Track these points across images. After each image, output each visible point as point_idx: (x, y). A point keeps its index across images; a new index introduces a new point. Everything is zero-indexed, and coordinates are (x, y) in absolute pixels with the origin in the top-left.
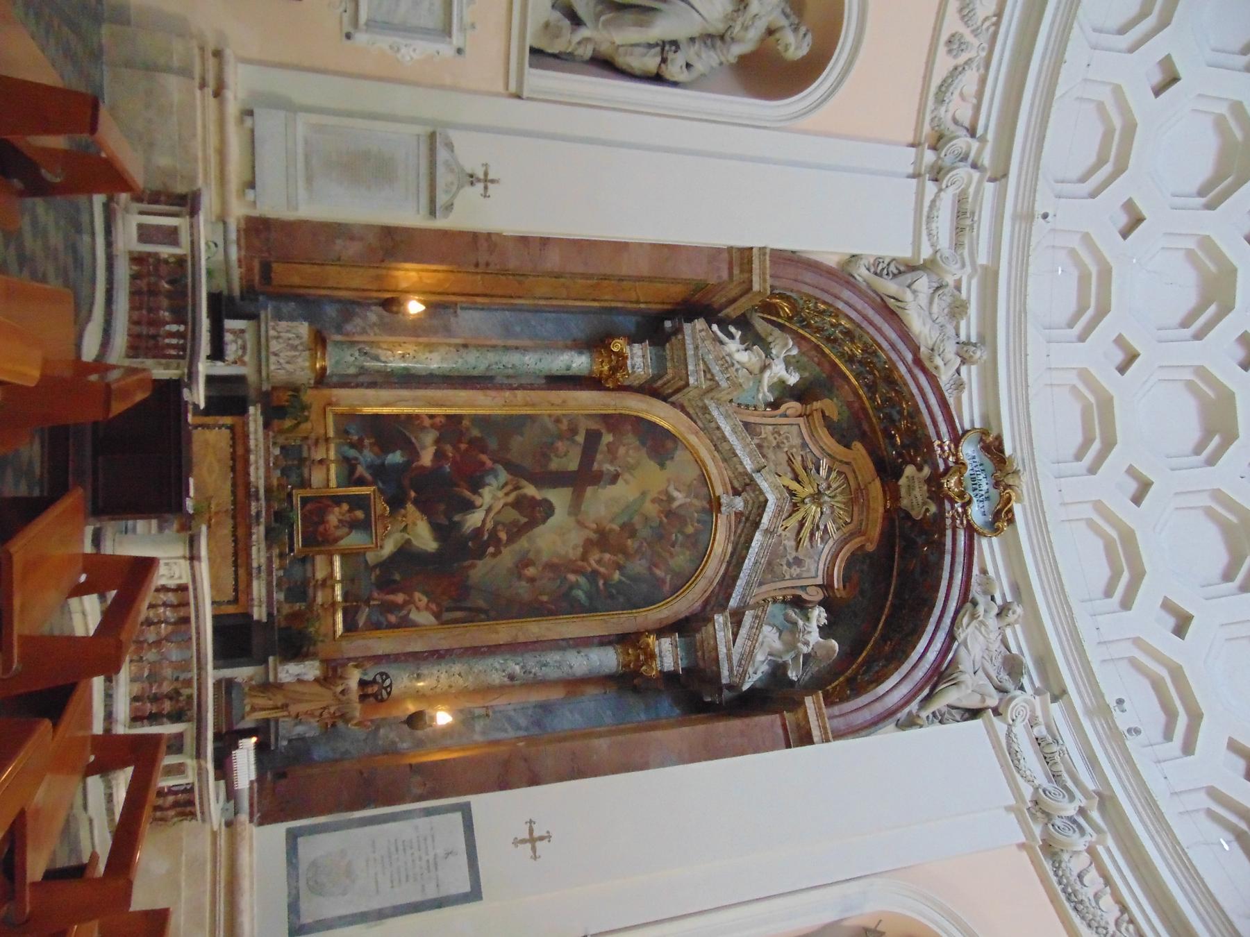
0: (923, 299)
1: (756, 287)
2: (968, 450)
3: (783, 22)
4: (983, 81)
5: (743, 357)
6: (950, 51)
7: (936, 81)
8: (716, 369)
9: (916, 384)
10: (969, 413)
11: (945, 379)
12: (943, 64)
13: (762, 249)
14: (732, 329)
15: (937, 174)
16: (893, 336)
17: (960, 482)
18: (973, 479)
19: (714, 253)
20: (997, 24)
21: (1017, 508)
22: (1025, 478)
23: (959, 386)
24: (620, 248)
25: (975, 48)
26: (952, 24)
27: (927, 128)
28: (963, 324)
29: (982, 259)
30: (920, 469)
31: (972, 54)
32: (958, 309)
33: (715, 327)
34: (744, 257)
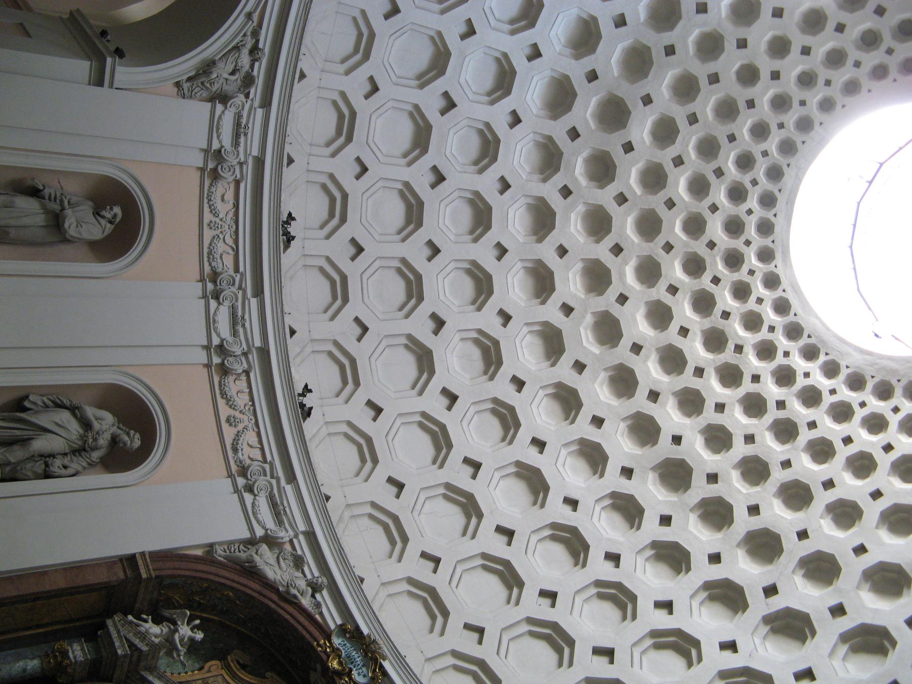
0: (272, 561)
1: (144, 576)
2: (337, 641)
3: (119, 431)
4: (259, 434)
5: (155, 629)
6: (231, 425)
7: (228, 442)
8: (136, 641)
9: (286, 612)
10: (332, 618)
11: (306, 602)
12: (229, 433)
13: (143, 554)
14: (145, 616)
15: (250, 489)
16: (257, 587)
17: (340, 663)
18: (349, 657)
19: (110, 563)
20: (253, 405)
21: (386, 665)
22: (380, 642)
23: (318, 605)
24: (41, 573)
25: (246, 420)
26: (225, 411)
27: (234, 468)
28: (306, 569)
29: (302, 527)
30: (315, 670)
31: (246, 423)
32: (299, 562)
33: (130, 617)
34: (131, 560)
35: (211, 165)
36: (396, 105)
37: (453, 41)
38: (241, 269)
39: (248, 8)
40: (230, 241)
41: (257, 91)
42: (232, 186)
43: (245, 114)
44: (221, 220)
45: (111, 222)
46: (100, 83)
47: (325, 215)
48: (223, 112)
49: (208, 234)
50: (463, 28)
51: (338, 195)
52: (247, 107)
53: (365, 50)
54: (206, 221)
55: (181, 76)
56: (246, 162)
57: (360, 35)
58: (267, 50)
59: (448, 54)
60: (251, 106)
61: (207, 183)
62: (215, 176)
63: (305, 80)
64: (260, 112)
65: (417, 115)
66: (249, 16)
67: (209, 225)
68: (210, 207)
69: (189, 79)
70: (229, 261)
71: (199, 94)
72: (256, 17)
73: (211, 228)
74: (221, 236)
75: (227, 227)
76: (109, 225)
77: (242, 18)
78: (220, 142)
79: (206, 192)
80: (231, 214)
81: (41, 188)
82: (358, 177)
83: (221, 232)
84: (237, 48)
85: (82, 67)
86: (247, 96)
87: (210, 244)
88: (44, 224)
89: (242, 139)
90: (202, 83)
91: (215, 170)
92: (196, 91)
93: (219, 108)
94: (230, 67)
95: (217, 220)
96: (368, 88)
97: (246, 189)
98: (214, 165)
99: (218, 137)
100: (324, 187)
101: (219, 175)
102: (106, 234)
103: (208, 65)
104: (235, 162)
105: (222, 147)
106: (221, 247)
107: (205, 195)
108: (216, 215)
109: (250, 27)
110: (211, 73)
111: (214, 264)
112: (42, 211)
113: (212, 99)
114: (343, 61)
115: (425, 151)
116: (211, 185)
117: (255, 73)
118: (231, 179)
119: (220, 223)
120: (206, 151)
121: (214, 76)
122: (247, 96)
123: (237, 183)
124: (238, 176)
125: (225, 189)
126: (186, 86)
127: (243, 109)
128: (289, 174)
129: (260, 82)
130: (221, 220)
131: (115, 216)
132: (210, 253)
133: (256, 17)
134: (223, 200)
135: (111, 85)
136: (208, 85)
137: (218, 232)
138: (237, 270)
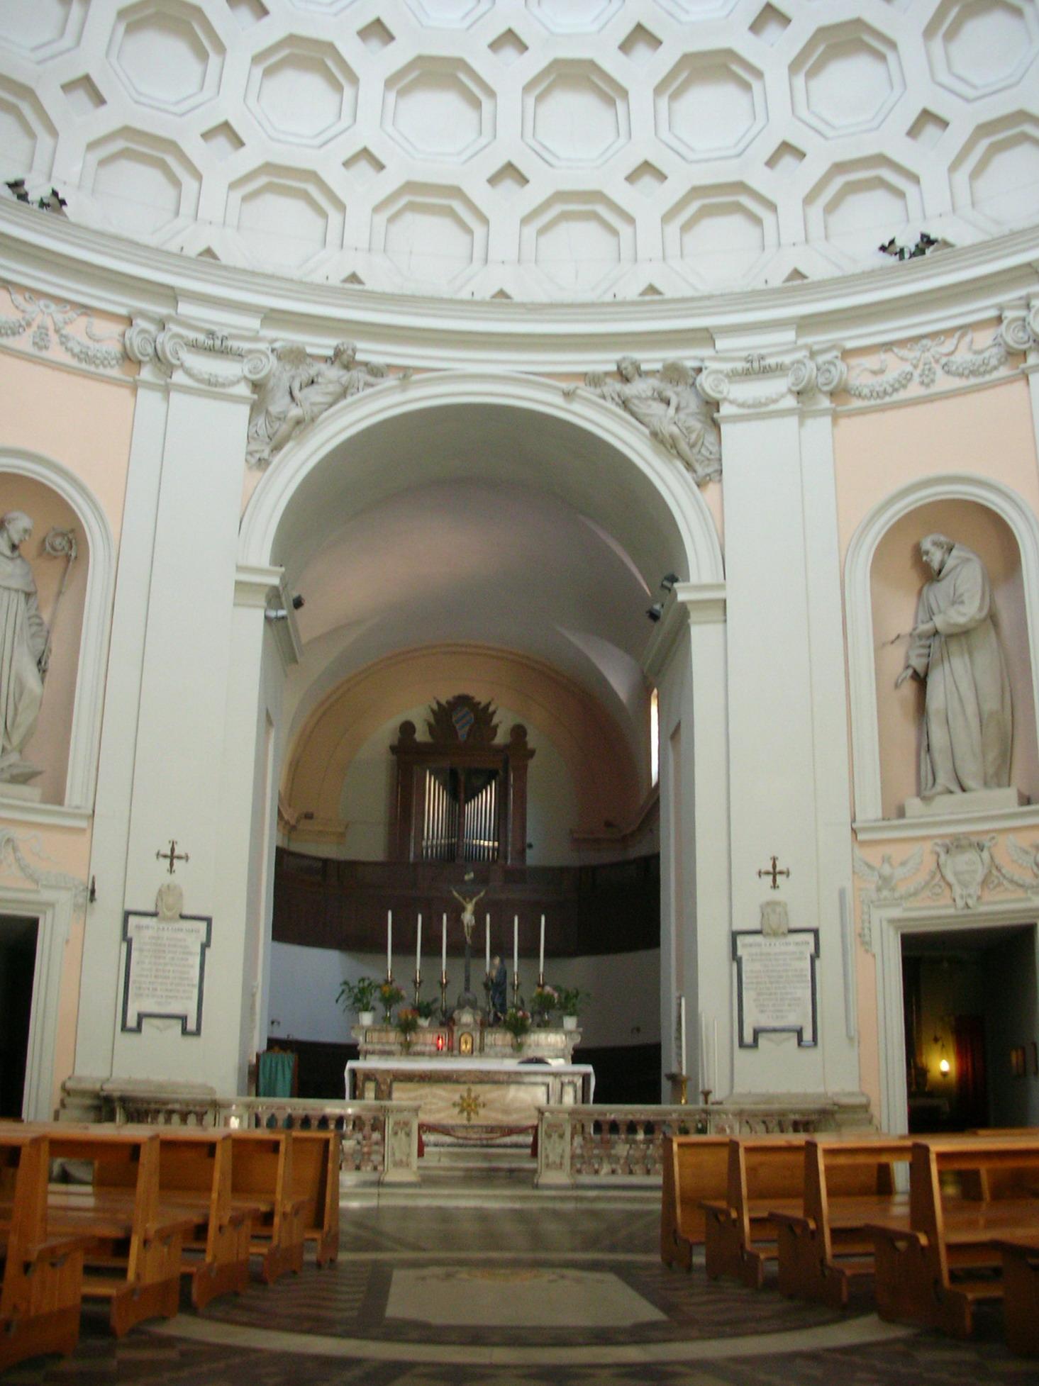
35: (825, 403)
36: (663, 125)
37: (533, 63)
38: (993, 313)
39: (559, 400)
40: (949, 345)
41: (687, 357)
42: (853, 362)
43: (727, 367)
44: (915, 367)
45: (950, 550)
47: (879, 195)
48: (732, 402)
49: (944, 383)
50: (509, 53)
51: (838, 182)
53: (586, 202)
54: (922, 391)
55: (686, 482)
56: (806, 346)
57: (565, 216)
58: (617, 356)
59: (557, 64)
61: (856, 403)
62: (840, 392)
63: (658, 285)
65: (672, 85)
66: (568, 395)
67: (928, 385)
68: (895, 390)
69: (689, 466)
70: (984, 338)
71: (711, 448)
72: (564, 385)
73: (933, 381)
74: (944, 360)
75: (927, 354)
76: (954, 552)
77: (576, 407)
78: (783, 396)
79: (872, 402)
80: (903, 352)
81: (910, 672)
82: (801, 155)
83: (937, 361)
84: (625, 404)
86: (699, 370)
87: (961, 375)
88: (967, 657)
89: (771, 361)
90: (692, 446)
91: (832, 394)
92: (707, 454)
93: (726, 410)
94: (658, 408)
95: (917, 373)
96: (647, 180)
97: (854, 337)
98: (826, 395)
99: (775, 401)
100: (831, 208)
101: (836, 387)
102: (971, 556)
103: (662, 442)
104: (811, 365)
105: (790, 391)
106: (963, 357)
107: (879, 401)
108: (908, 377)
109: (585, 391)
110: (672, 436)
111: (994, 362)
112: (946, 665)
113: (716, 425)
114: (614, 232)
115: (730, 54)
116: (859, 396)
117: (658, 366)
118: (841, 366)
119: (921, 367)
120: (803, 415)
121: (675, 430)
122: (699, 370)
123: (846, 354)
124: (836, 353)
125: (860, 374)
126: (701, 470)
127: (720, 372)
128: (817, 270)
129: (671, 355)
130: (915, 367)
131: (935, 544)
132: (973, 373)
133: (564, 385)
134: (882, 371)
135: (721, 587)
137: (939, 371)
138: (999, 320)
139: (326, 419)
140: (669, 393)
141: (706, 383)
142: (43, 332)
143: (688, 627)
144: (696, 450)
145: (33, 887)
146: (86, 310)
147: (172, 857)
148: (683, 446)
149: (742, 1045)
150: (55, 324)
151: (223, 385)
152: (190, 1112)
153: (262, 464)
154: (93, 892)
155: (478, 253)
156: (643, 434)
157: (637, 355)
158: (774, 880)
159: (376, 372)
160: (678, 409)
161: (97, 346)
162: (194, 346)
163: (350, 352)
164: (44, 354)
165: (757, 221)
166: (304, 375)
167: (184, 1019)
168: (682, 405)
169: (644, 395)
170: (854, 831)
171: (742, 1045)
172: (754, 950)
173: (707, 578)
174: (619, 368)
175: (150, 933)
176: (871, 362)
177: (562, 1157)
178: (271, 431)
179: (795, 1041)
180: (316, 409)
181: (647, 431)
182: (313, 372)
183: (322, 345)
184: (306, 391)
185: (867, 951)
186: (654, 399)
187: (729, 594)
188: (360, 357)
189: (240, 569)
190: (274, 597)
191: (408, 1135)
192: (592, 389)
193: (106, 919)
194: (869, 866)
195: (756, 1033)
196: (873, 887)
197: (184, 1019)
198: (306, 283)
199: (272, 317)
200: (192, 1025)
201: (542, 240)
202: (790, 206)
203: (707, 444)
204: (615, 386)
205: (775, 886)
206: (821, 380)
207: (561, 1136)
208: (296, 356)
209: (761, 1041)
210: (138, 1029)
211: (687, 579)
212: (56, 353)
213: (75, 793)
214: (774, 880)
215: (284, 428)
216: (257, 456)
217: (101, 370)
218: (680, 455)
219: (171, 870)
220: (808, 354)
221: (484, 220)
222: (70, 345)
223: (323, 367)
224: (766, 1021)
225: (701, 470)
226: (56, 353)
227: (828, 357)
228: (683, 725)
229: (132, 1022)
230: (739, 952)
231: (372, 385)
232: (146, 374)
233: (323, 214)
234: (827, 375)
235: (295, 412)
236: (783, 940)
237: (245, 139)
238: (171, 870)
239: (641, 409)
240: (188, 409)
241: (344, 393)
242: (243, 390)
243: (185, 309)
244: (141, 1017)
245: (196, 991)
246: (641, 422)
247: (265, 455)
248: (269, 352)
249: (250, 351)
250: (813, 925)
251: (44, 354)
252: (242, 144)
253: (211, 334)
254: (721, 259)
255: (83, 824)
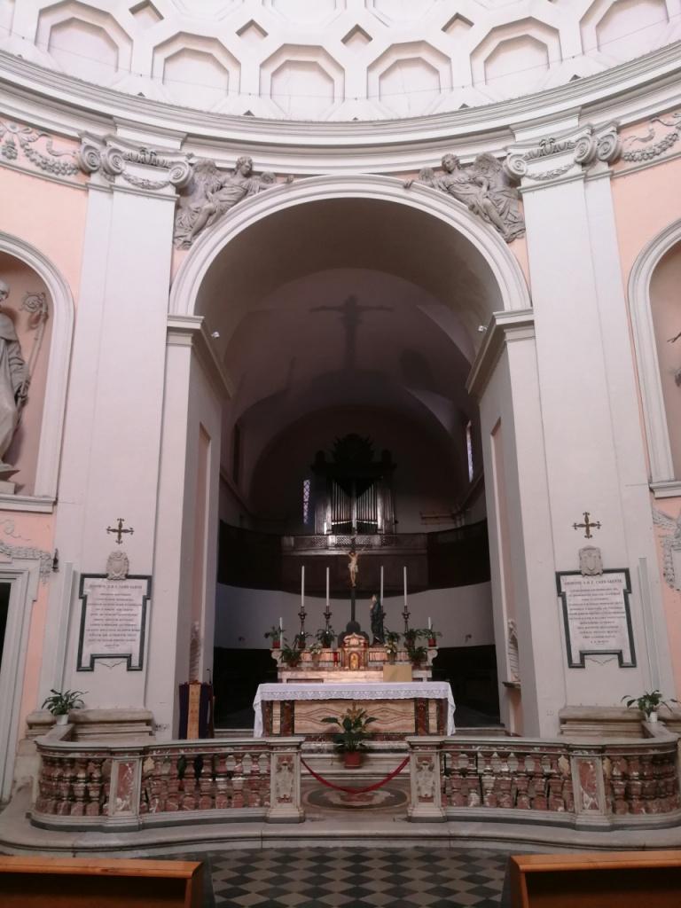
35: (604, 167)
39: (401, 192)
41: (494, 149)
42: (626, 134)
43: (524, 152)
46: (531, 323)
48: (529, 177)
52: (514, 151)
57: (398, 63)
58: (440, 155)
60: (515, 146)
64: (521, 136)
66: (407, 187)
68: (665, 150)
69: (499, 228)
72: (405, 180)
78: (570, 167)
84: (449, 189)
85: (516, 351)
86: (503, 159)
89: (560, 142)
92: (513, 220)
93: (525, 183)
94: (473, 189)
97: (625, 114)
98: (602, 161)
99: (565, 171)
110: (485, 206)
113: (520, 198)
116: (633, 160)
120: (586, 179)
121: (488, 202)
125: (631, 143)
127: (521, 155)
134: (651, 138)
135: (530, 311)
136: (502, 206)
139: (231, 214)
140: (481, 178)
141: (511, 164)
142: (11, 146)
143: (505, 344)
144: (503, 217)
145: (9, 560)
146: (47, 132)
147: (120, 531)
148: (494, 214)
149: (571, 665)
150: (20, 141)
151: (154, 188)
152: (89, 760)
153: (187, 244)
154: (56, 561)
155: (338, 93)
156: (463, 209)
157: (458, 153)
158: (588, 531)
159: (268, 179)
160: (488, 188)
161: (56, 159)
162: (130, 160)
163: (247, 164)
164: (12, 162)
165: (542, 46)
166: (215, 182)
167: (129, 657)
168: (492, 185)
169: (463, 181)
170: (651, 490)
171: (571, 665)
172: (577, 587)
173: (517, 306)
174: (443, 162)
175: (101, 590)
176: (642, 131)
177: (433, 789)
178: (192, 221)
179: (617, 661)
180: (224, 204)
181: (466, 207)
182: (221, 179)
183: (227, 159)
184: (217, 194)
185: (672, 587)
186: (471, 183)
187: (535, 317)
188: (256, 169)
189: (170, 318)
190: (196, 335)
191: (290, 770)
192: (424, 182)
193: (60, 584)
194: (670, 518)
195: (583, 655)
196: (672, 533)
197: (129, 657)
198: (212, 114)
199: (188, 139)
200: (135, 662)
201: (383, 82)
202: (569, 30)
203: (511, 211)
204: (441, 177)
205: (588, 536)
206: (601, 151)
207: (431, 769)
208: (210, 168)
209: (588, 662)
210: (91, 668)
211: (502, 308)
212: (23, 161)
213: (43, 485)
214: (588, 531)
215: (200, 218)
216: (182, 239)
217: (60, 176)
218: (492, 221)
219: (119, 542)
220: (590, 132)
221: (342, 69)
222: (33, 156)
223: (228, 175)
224: (590, 646)
225: (508, 230)
226: (23, 161)
227: (607, 132)
228: (502, 422)
229: (86, 663)
230: (563, 590)
231: (264, 189)
232: (95, 179)
233: (226, 71)
234: (606, 146)
235: (208, 206)
236: (597, 578)
237: (164, 16)
238: (119, 542)
239: (461, 190)
240: (125, 203)
241: (246, 193)
242: (170, 191)
243: (122, 133)
244: (93, 658)
245: (139, 634)
246: (462, 201)
247: (188, 238)
248: (187, 164)
249: (173, 163)
250: (624, 567)
251: (12, 162)
252: (161, 18)
253: (143, 150)
254: (519, 74)
255: (48, 509)
